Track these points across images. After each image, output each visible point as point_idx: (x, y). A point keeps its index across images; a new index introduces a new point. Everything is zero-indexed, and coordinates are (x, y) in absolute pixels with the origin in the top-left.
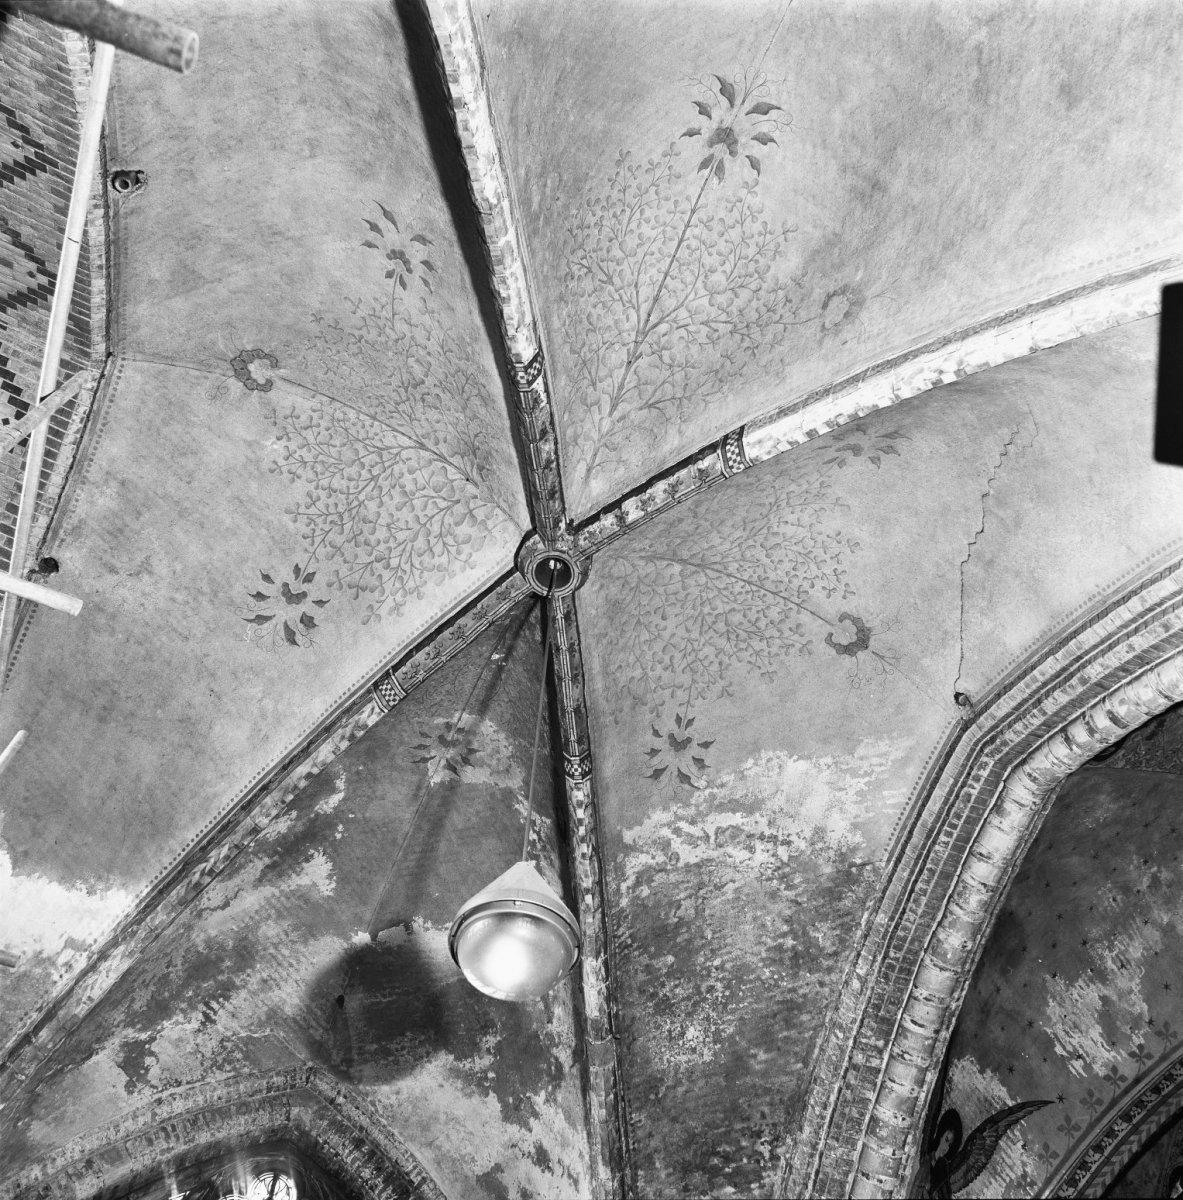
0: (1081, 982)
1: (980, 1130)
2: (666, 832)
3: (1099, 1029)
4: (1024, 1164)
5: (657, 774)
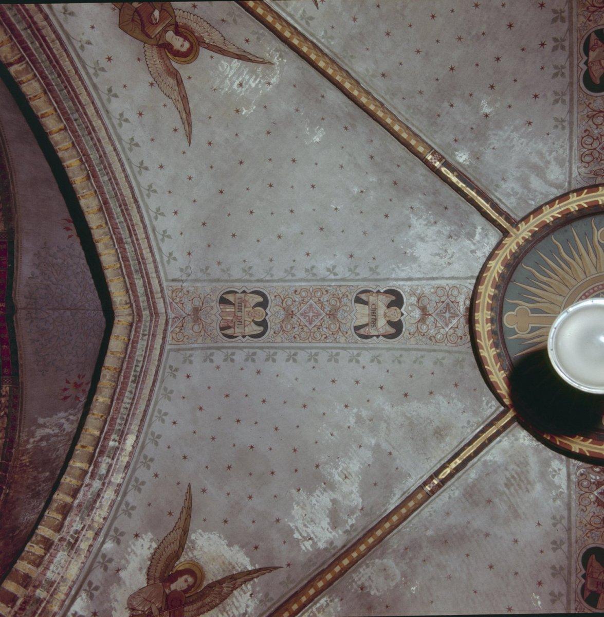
0: (318, 492)
1: (220, 582)
2: (63, 421)
3: (328, 520)
4: (247, 606)
5: (65, 398)
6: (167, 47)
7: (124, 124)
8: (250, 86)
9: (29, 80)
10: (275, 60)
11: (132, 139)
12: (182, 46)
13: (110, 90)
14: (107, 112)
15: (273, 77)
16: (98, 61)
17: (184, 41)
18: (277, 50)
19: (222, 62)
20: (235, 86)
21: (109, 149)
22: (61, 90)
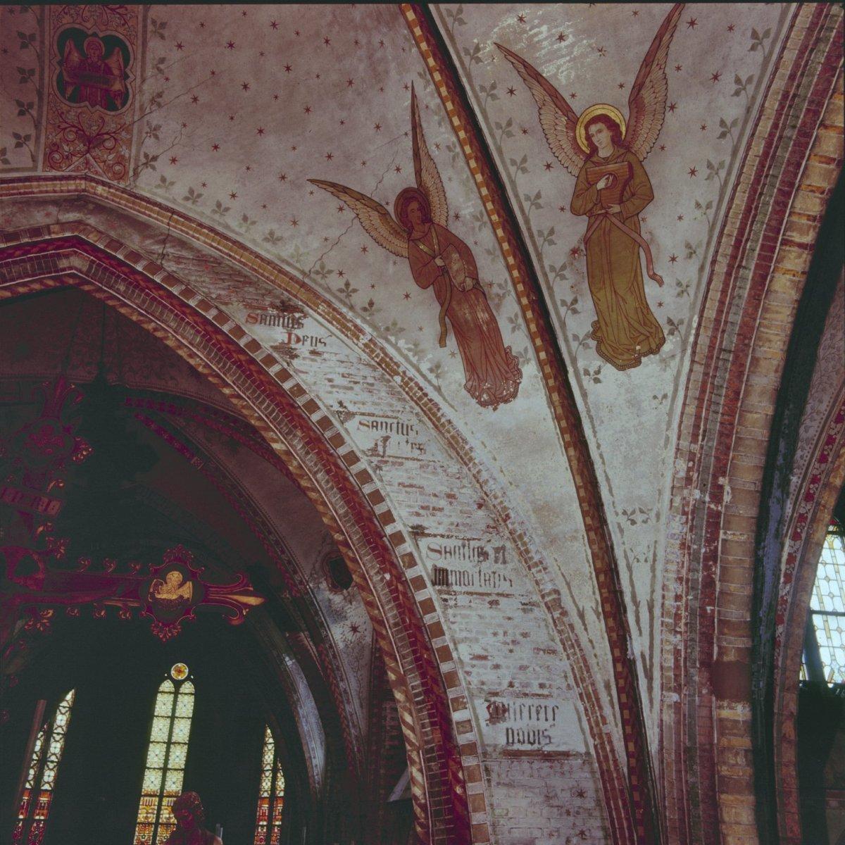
6: (616, 140)
7: (744, 79)
8: (549, 30)
9: (800, 214)
10: (489, 47)
11: (753, 48)
12: (600, 131)
13: (723, 135)
14: (748, 110)
15: (509, 25)
16: (706, 179)
17: (593, 136)
18: (478, 60)
19: (564, 82)
20: (570, 39)
21: (790, 56)
22: (775, 177)
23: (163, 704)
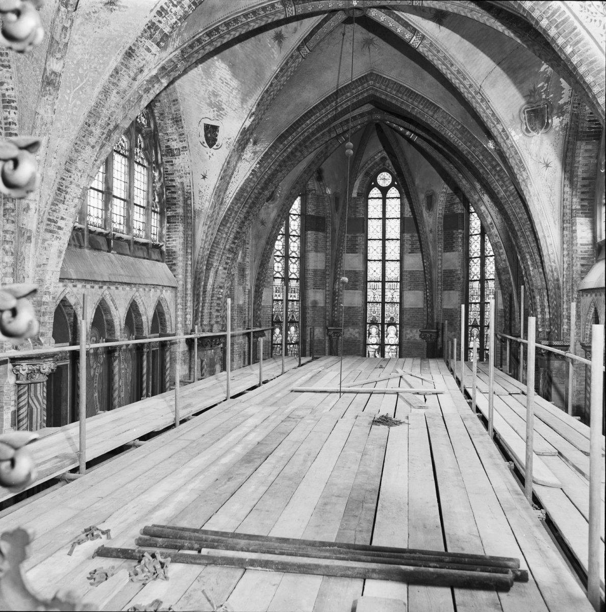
23: (374, 208)
